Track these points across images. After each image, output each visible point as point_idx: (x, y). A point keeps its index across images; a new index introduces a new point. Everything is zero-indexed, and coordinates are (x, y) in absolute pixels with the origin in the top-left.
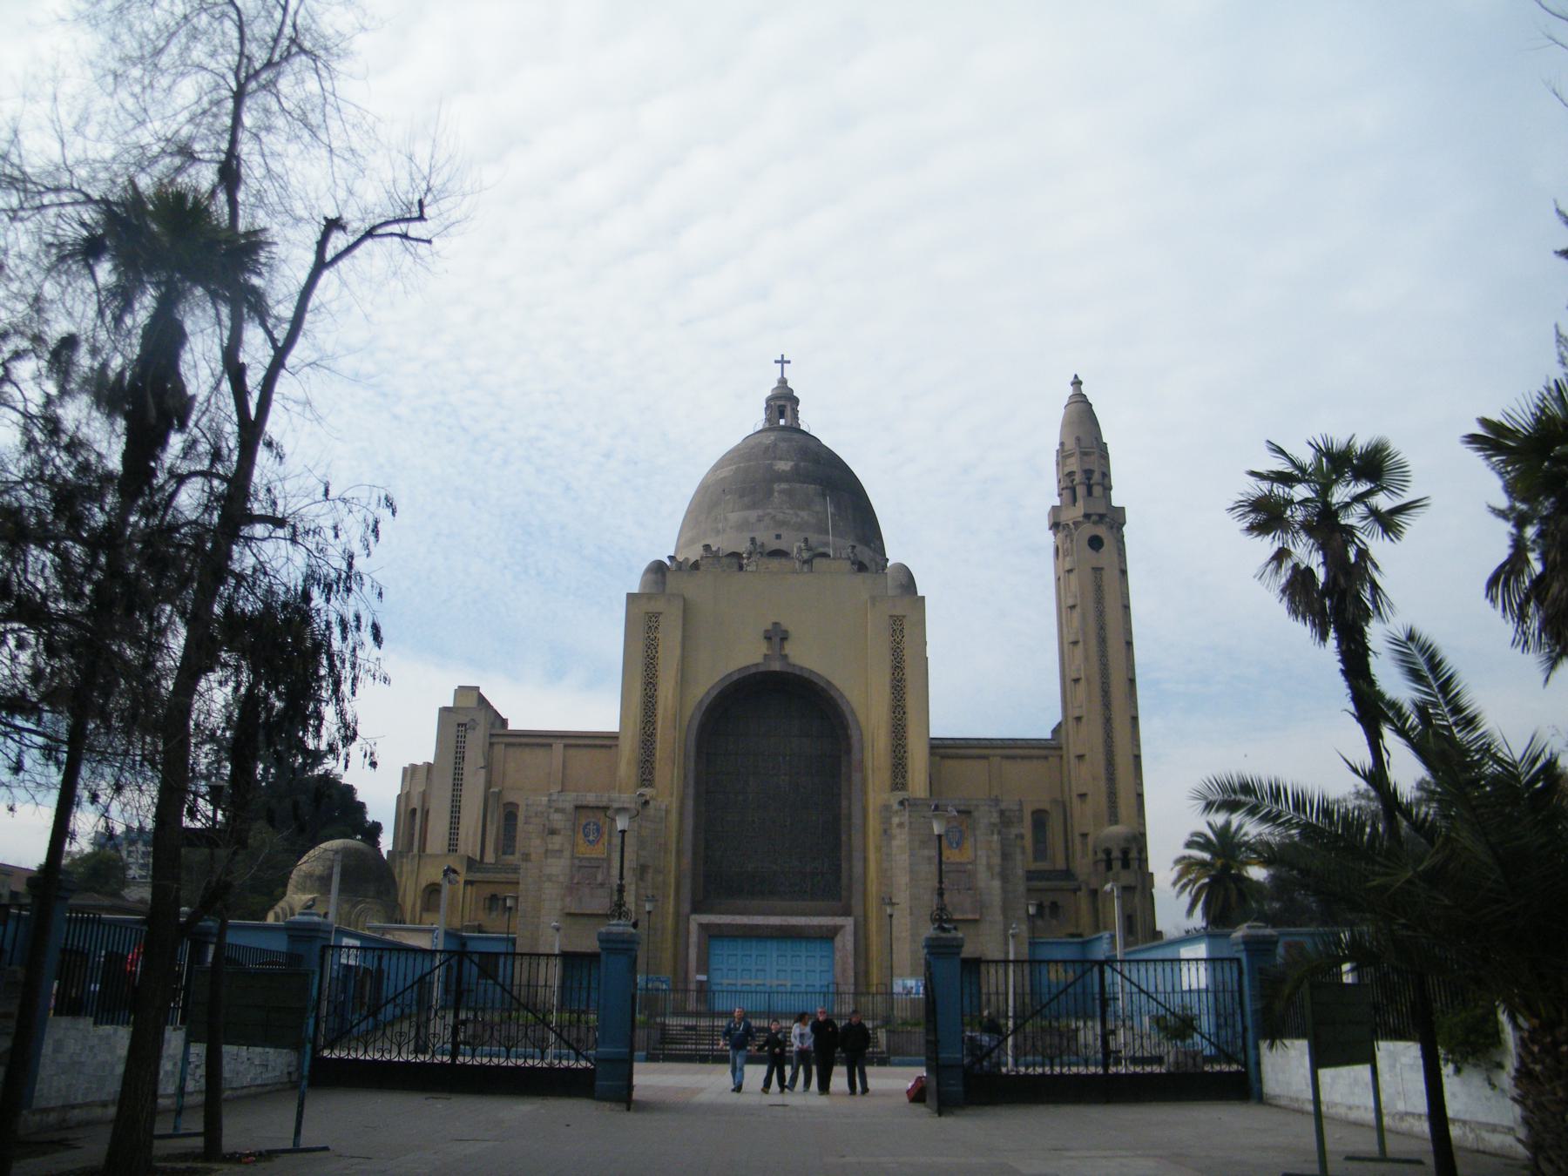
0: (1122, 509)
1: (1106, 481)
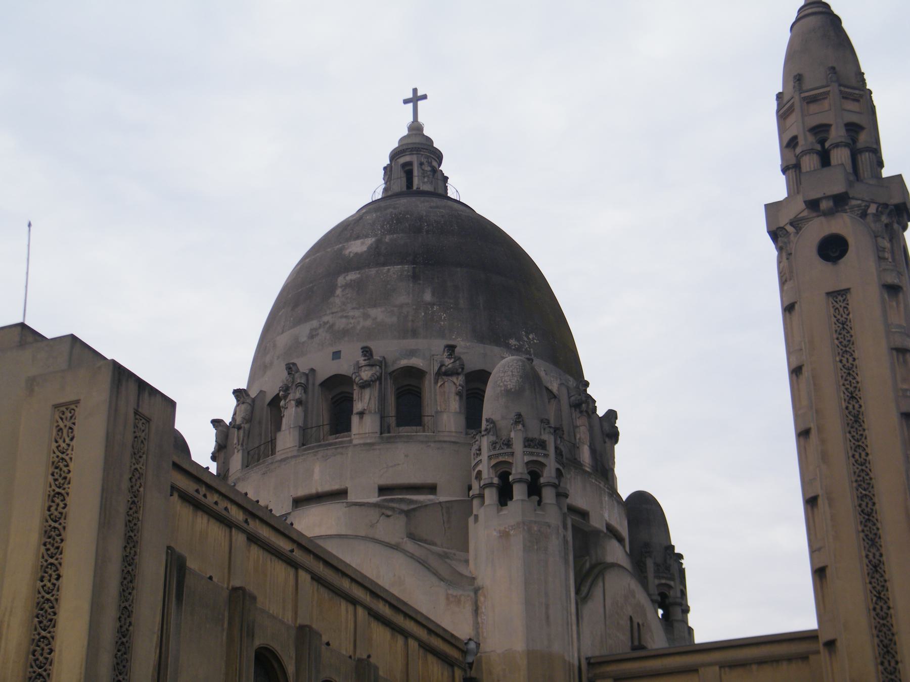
0: (899, 178)
1: (863, 139)
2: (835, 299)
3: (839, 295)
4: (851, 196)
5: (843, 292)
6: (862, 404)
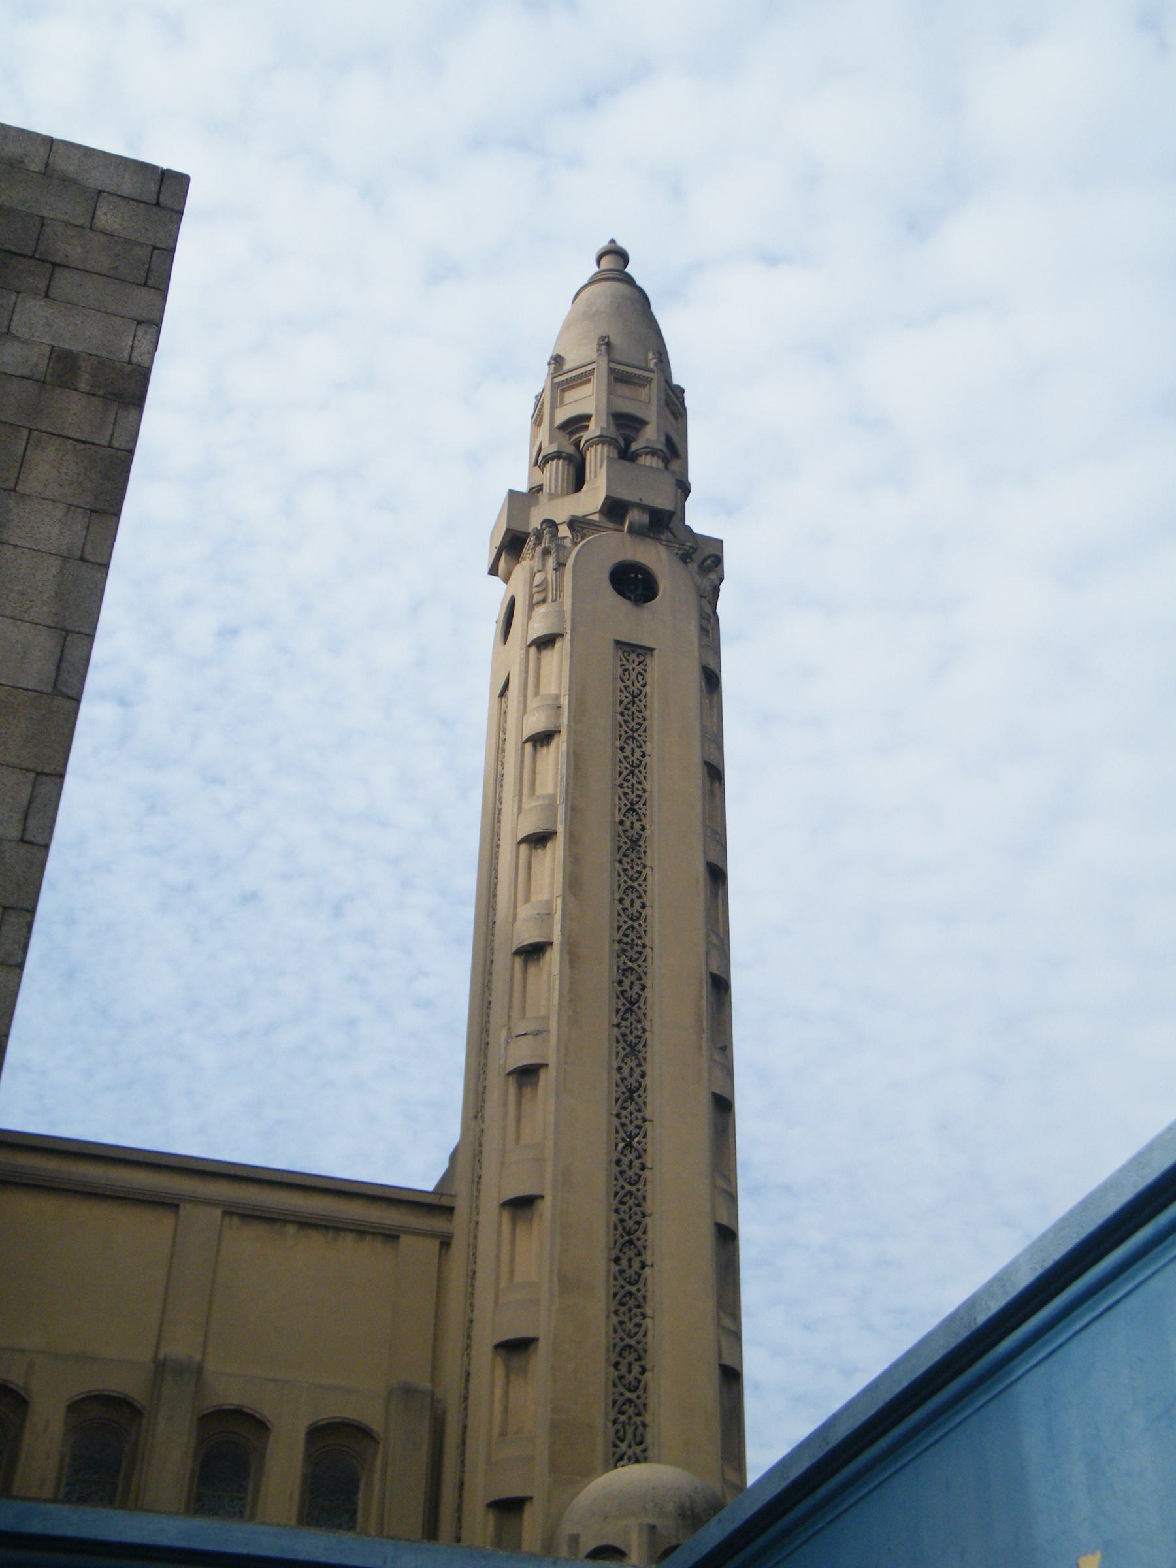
2: (626, 654)
4: (670, 526)
5: (639, 651)
6: (647, 826)
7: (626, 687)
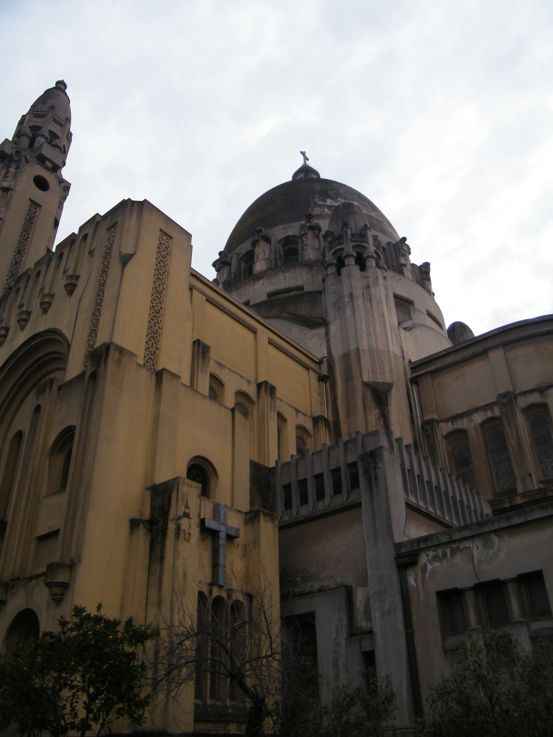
3: (35, 205)
5: (36, 205)
7: (29, 215)
